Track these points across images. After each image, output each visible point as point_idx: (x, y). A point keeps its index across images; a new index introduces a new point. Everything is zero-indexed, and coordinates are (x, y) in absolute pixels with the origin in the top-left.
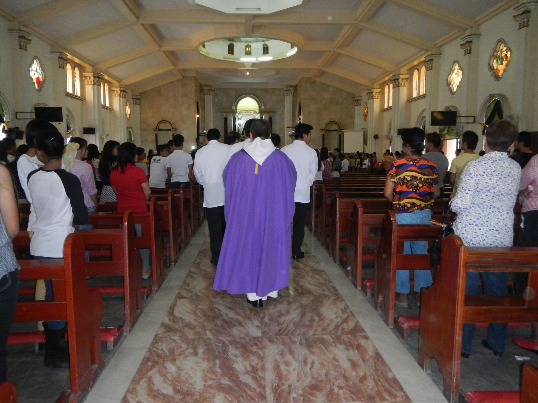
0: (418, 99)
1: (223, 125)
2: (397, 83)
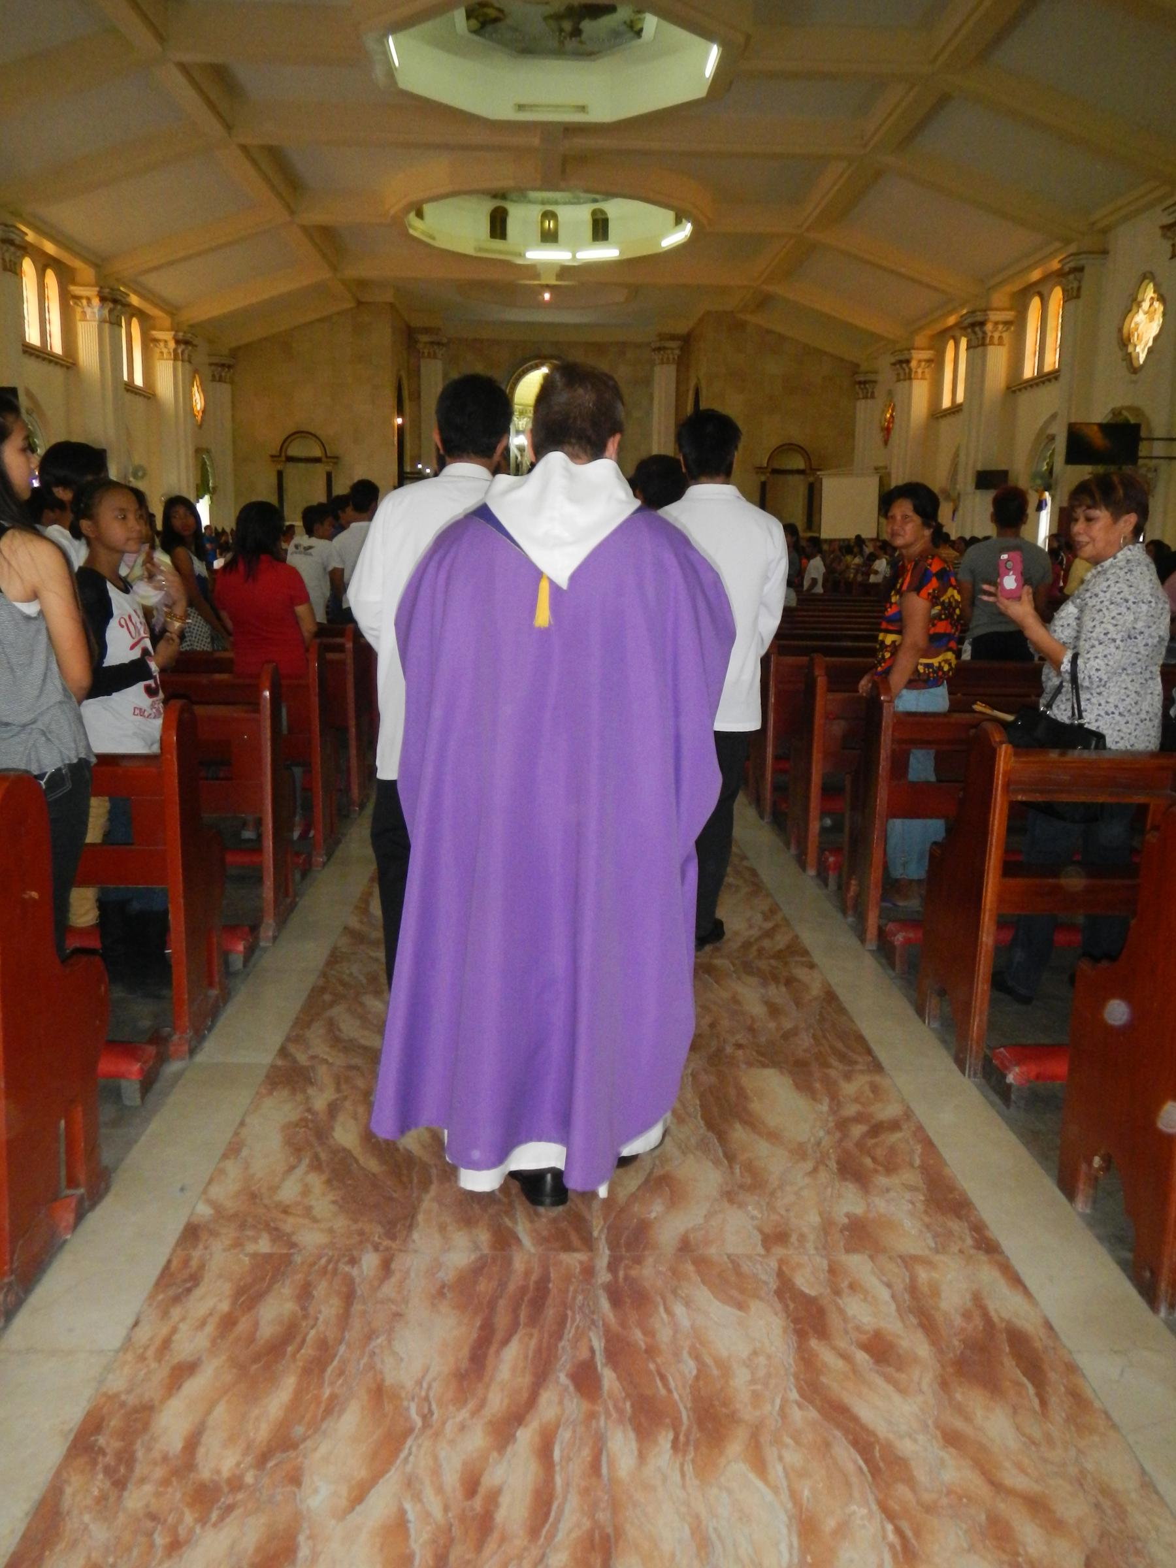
0: (1037, 384)
2: (980, 335)
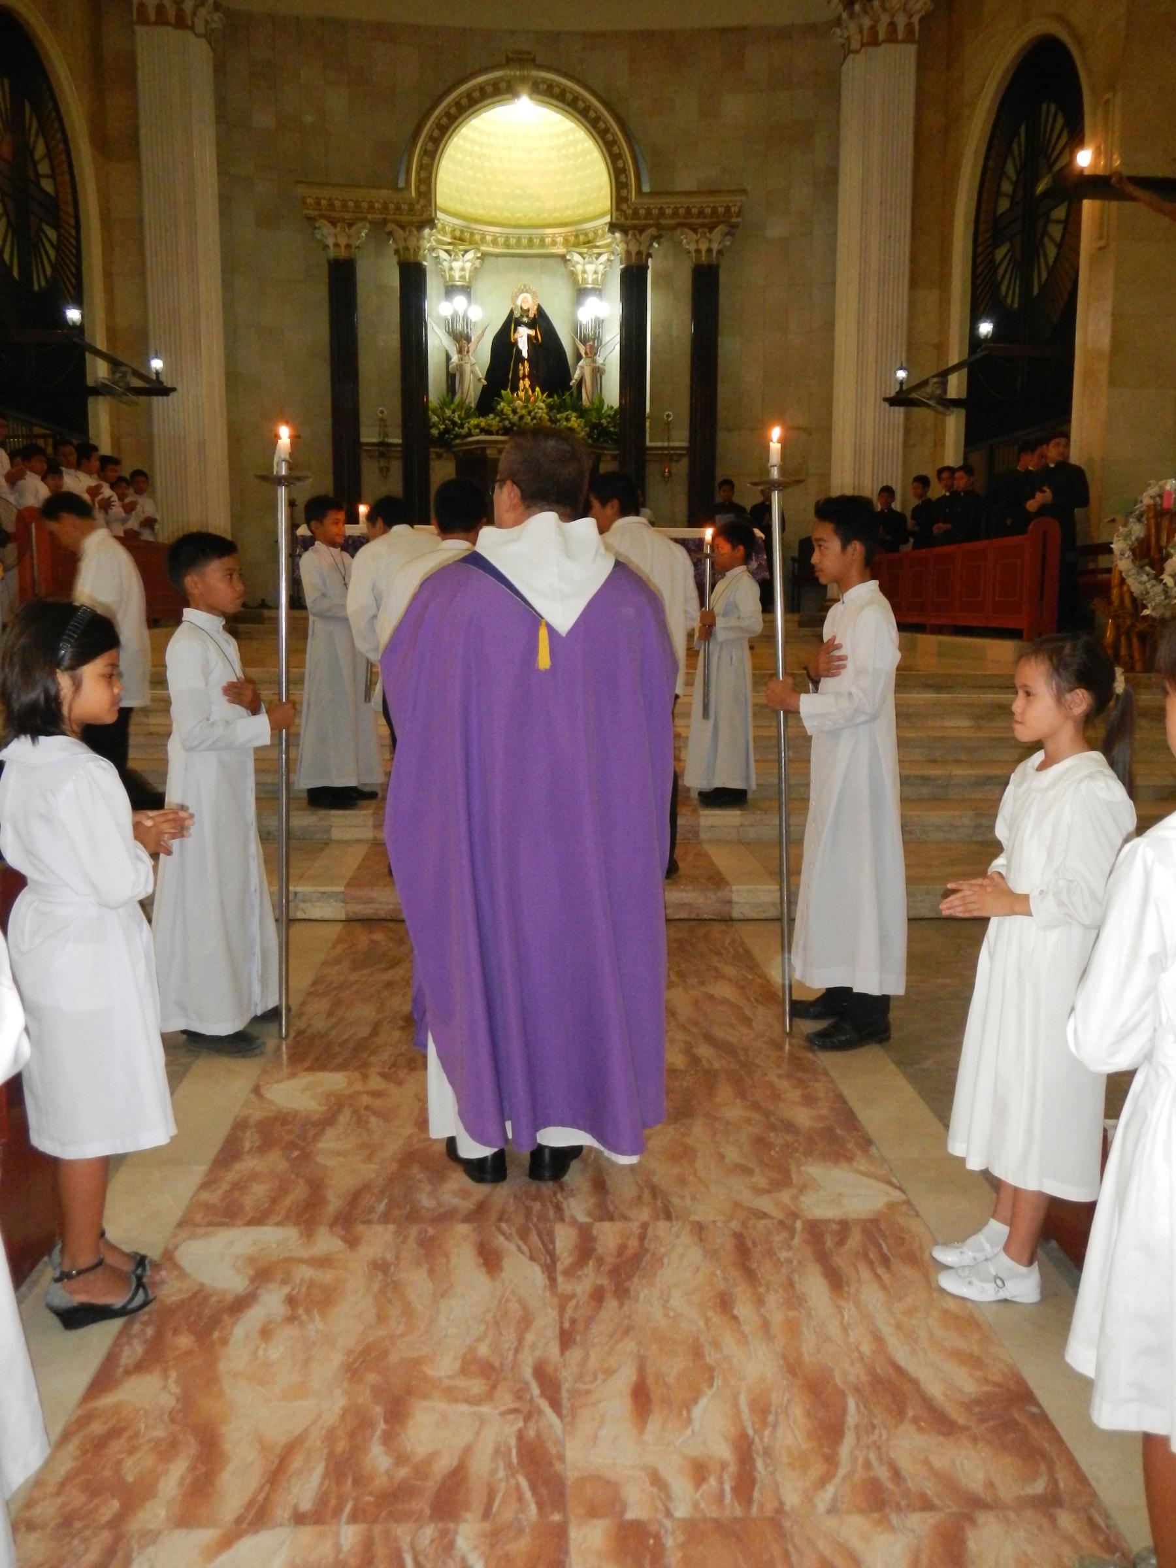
1: (319, 330)
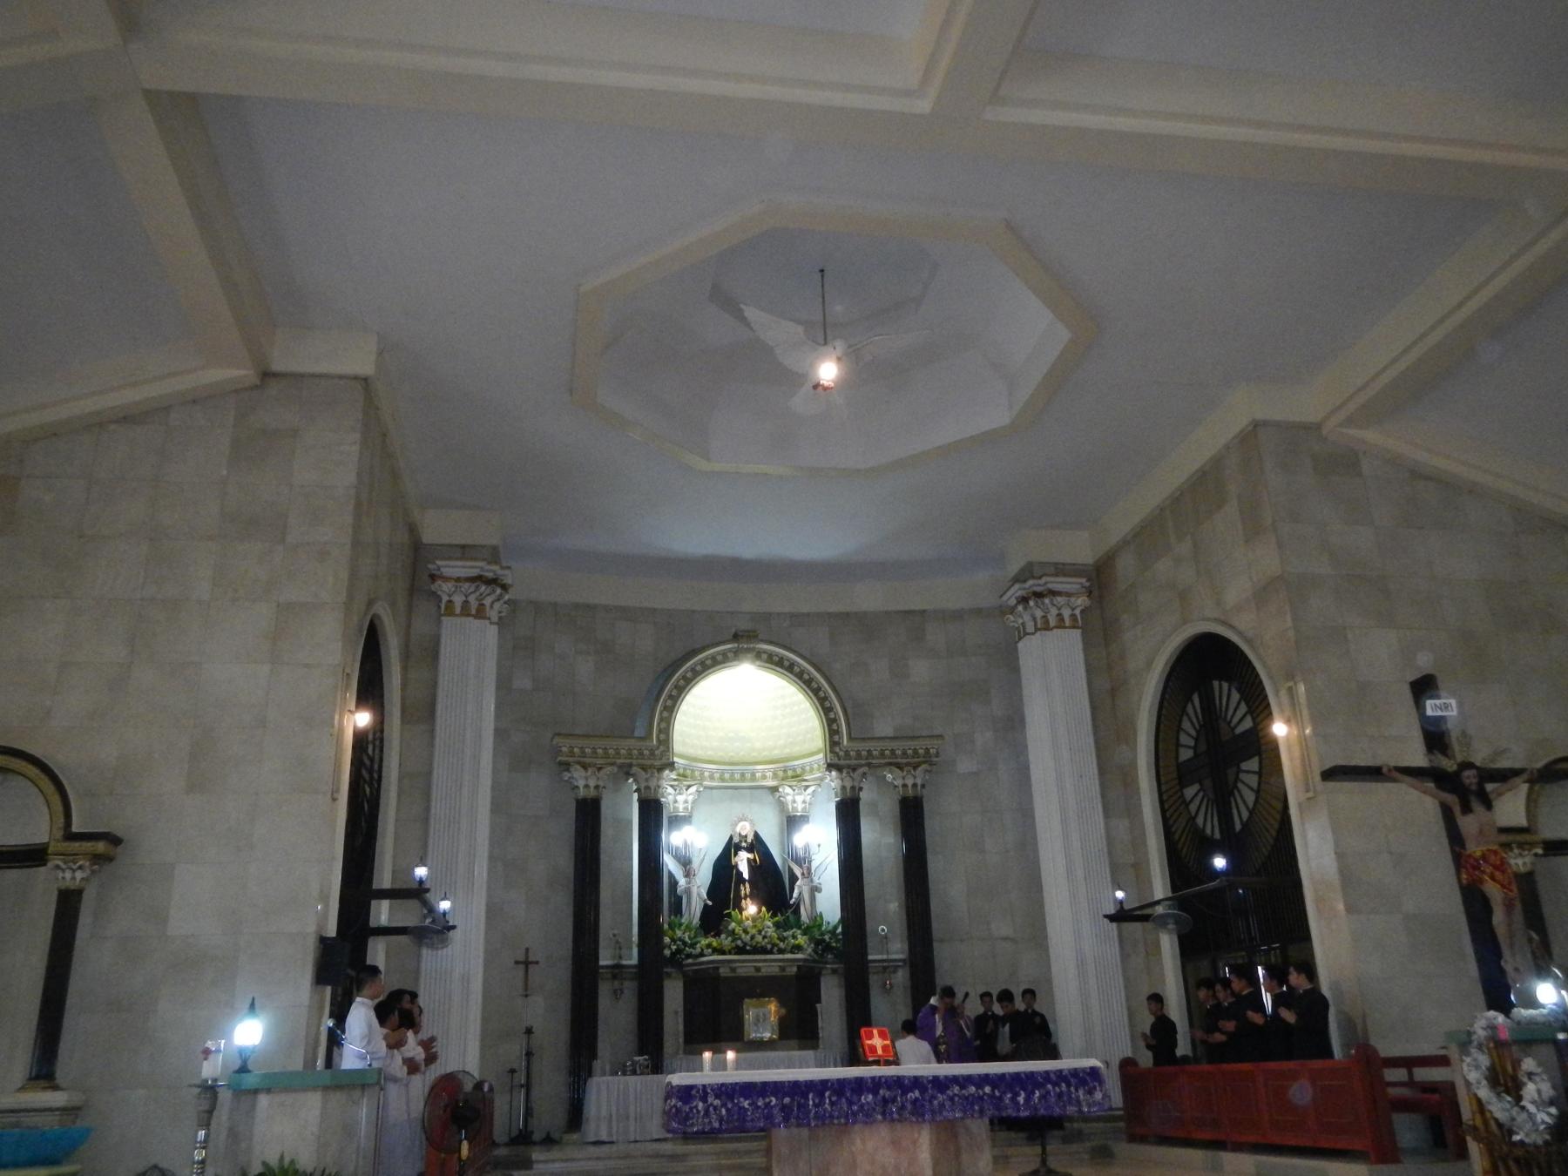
1: (564, 860)
